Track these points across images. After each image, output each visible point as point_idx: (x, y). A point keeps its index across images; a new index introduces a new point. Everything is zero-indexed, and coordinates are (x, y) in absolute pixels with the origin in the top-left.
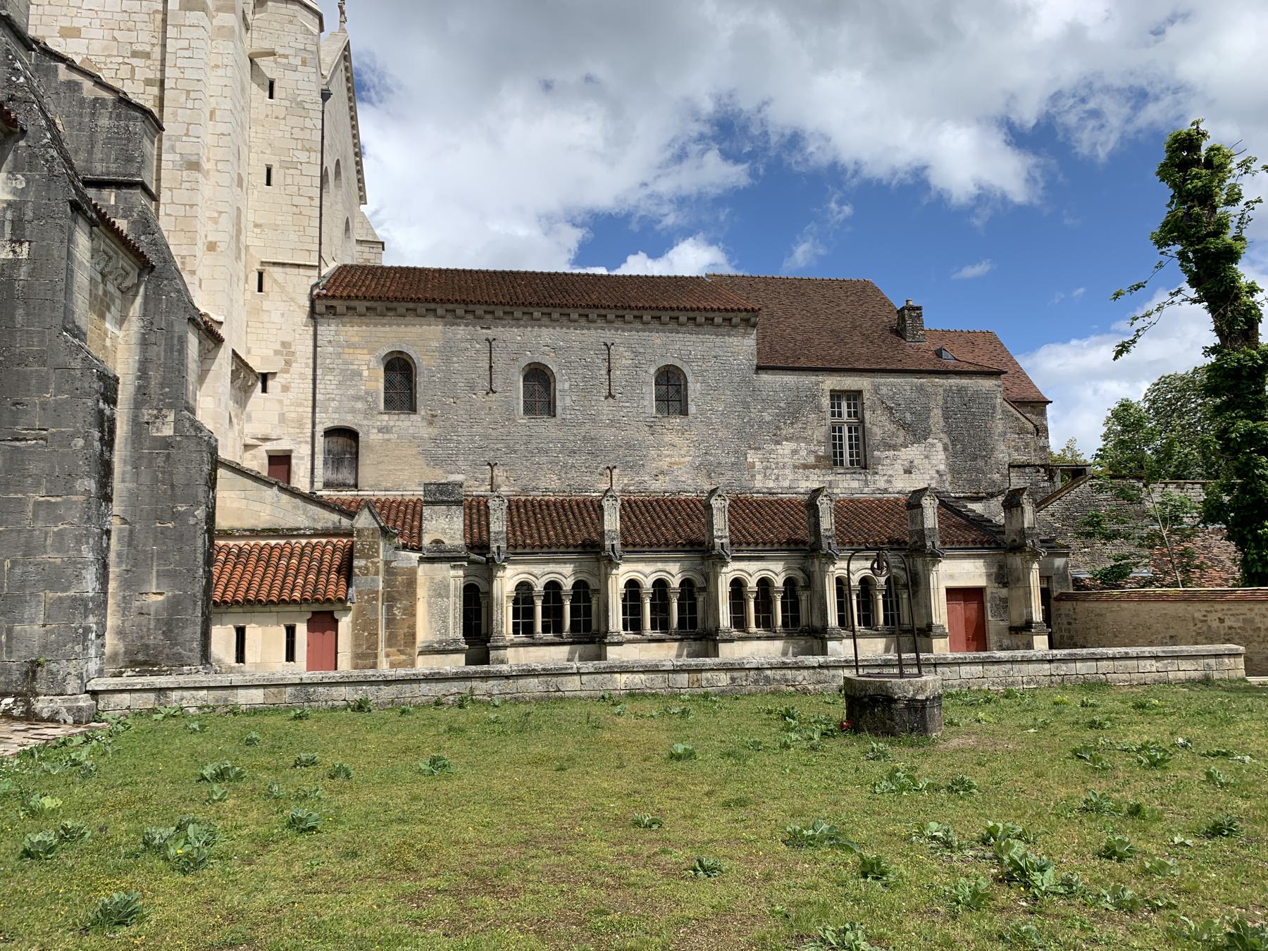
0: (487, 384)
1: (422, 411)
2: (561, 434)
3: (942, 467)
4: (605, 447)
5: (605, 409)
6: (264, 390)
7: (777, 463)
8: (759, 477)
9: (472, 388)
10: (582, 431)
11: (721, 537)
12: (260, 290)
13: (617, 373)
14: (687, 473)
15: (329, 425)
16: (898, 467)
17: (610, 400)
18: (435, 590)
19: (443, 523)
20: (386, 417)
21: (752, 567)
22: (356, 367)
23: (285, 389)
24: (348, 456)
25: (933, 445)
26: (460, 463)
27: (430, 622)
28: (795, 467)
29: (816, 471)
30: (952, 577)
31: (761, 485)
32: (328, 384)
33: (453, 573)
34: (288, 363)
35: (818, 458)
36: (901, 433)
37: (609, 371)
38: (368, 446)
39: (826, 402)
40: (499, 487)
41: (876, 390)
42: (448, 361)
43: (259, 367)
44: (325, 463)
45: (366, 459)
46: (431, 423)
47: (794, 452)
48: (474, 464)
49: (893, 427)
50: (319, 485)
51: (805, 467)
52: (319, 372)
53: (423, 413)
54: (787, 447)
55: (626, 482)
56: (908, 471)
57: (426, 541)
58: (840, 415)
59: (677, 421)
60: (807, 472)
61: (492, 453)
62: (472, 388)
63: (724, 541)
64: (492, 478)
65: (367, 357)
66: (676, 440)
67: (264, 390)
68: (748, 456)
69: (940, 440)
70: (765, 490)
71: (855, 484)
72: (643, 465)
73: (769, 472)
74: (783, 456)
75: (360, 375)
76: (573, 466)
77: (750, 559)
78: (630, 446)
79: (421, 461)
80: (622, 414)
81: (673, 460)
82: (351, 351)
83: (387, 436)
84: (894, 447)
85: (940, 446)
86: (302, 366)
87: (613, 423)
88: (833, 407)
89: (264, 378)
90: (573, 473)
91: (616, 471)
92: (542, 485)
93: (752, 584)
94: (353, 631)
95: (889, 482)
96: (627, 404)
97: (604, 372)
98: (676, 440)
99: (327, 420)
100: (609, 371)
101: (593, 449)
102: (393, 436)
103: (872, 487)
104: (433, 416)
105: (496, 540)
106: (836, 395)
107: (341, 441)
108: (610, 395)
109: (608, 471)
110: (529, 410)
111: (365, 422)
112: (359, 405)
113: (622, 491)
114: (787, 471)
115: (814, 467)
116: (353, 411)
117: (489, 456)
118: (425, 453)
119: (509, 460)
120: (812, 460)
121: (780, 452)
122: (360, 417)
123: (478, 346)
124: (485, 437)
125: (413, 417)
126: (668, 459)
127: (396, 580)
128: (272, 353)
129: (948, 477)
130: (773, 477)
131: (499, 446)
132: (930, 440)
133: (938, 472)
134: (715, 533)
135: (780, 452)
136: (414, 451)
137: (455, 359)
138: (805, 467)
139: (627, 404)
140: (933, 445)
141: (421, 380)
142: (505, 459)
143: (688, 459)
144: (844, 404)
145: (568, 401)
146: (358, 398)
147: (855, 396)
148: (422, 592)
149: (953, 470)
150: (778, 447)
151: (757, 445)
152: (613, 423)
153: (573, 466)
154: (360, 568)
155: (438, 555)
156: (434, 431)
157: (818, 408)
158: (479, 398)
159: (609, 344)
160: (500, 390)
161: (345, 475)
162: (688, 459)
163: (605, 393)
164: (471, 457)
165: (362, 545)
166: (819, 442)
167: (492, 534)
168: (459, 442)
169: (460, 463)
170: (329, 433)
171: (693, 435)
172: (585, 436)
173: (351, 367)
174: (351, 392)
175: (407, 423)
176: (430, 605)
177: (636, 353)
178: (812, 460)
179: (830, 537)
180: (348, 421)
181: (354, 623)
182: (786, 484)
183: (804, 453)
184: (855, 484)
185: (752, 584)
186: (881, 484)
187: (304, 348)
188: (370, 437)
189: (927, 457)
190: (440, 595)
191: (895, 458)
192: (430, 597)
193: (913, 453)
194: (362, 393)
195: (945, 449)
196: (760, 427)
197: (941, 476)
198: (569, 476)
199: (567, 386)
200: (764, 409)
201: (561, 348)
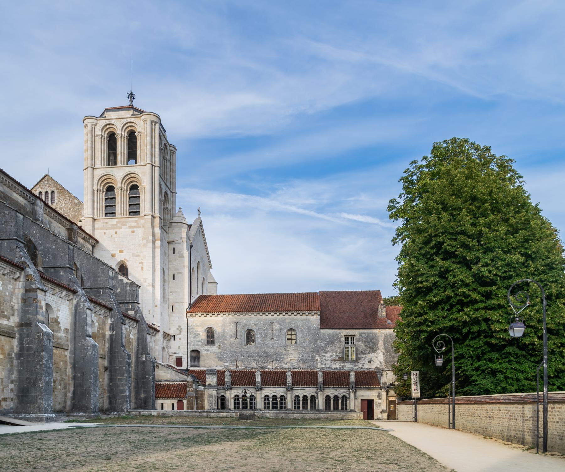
0: (235, 336)
2: (257, 351)
3: (382, 361)
5: (271, 343)
6: (174, 340)
8: (319, 364)
10: (263, 350)
12: (173, 311)
13: (274, 332)
15: (192, 349)
16: (367, 360)
17: (273, 340)
20: (206, 347)
21: (301, 392)
23: (180, 339)
25: (379, 353)
28: (331, 361)
29: (338, 362)
30: (363, 396)
32: (191, 337)
33: (214, 392)
34: (180, 332)
35: (339, 358)
36: (368, 349)
38: (202, 355)
39: (343, 339)
40: (238, 367)
41: (360, 334)
43: (171, 333)
44: (191, 360)
45: (202, 359)
46: (219, 348)
47: (331, 356)
48: (231, 360)
49: (365, 347)
50: (189, 366)
51: (335, 360)
52: (189, 334)
53: (217, 345)
54: (329, 354)
56: (370, 362)
57: (207, 384)
58: (348, 343)
60: (335, 362)
65: (202, 329)
66: (293, 352)
67: (174, 340)
69: (382, 351)
71: (351, 366)
73: (322, 362)
74: (328, 357)
75: (199, 334)
76: (260, 361)
77: (301, 390)
78: (278, 354)
79: (217, 360)
83: (207, 352)
84: (365, 354)
85: (381, 354)
86: (184, 332)
87: (273, 347)
88: (346, 340)
89: (174, 336)
91: (274, 362)
92: (251, 366)
93: (301, 397)
95: (363, 365)
97: (270, 331)
98: (293, 352)
99: (192, 348)
101: (267, 355)
102: (209, 352)
103: (357, 367)
106: (346, 337)
107: (195, 354)
108: (272, 339)
111: (201, 348)
112: (200, 343)
113: (276, 368)
114: (329, 362)
115: (338, 360)
116: (198, 345)
118: (218, 357)
120: (337, 358)
121: (327, 356)
122: (200, 347)
124: (235, 352)
126: (290, 358)
128: (176, 329)
129: (384, 364)
132: (378, 352)
133: (380, 362)
135: (327, 356)
136: (215, 356)
138: (335, 360)
140: (379, 353)
142: (240, 359)
143: (297, 358)
144: (350, 339)
145: (259, 341)
146: (199, 341)
147: (353, 337)
148: (206, 397)
149: (386, 362)
152: (273, 347)
155: (210, 387)
156: (220, 351)
157: (340, 341)
158: (233, 340)
161: (196, 363)
163: (270, 337)
166: (340, 353)
168: (227, 354)
170: (192, 351)
171: (298, 350)
174: (197, 340)
175: (213, 348)
176: (208, 400)
177: (281, 325)
178: (337, 358)
180: (197, 348)
181: (187, 403)
182: (328, 366)
183: (335, 356)
184: (351, 366)
185: (301, 397)
186: (360, 366)
187: (184, 328)
188: (203, 353)
189: (377, 357)
190: (210, 398)
191: (366, 358)
193: (372, 356)
195: (384, 354)
196: (320, 348)
197: (381, 363)
199: (259, 336)
201: (257, 324)
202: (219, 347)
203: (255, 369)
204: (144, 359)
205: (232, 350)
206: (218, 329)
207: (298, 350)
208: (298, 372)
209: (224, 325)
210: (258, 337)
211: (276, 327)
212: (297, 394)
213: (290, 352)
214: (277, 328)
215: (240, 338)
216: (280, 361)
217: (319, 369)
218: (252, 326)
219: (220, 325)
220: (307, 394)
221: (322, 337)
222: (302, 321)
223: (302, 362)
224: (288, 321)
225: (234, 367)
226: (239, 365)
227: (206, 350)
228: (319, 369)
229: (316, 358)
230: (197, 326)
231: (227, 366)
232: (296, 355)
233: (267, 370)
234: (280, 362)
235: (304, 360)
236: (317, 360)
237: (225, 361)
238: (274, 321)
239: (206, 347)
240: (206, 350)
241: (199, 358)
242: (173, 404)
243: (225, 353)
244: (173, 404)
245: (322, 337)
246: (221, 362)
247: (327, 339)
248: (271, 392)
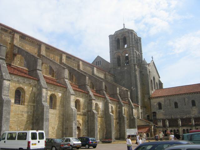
42: (165, 103)
45: (157, 116)
108: (185, 105)
116: (155, 110)
141: (162, 106)
202: (164, 110)
204: (132, 118)
206: (163, 103)
209: (165, 101)
219: (163, 101)
227: (159, 112)
239: (159, 111)
240: (159, 112)
241: (156, 115)
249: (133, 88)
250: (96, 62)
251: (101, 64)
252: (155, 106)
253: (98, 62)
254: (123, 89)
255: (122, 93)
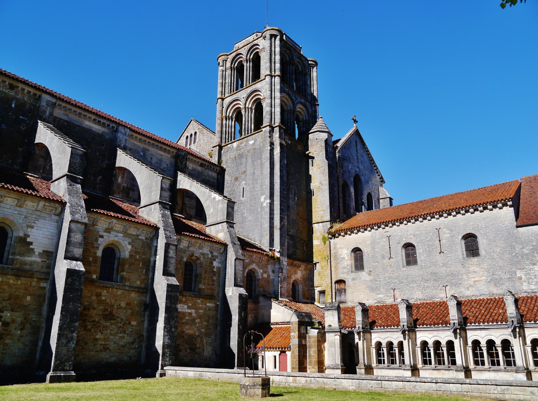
1: (366, 269)
2: (421, 273)
4: (441, 276)
5: (440, 258)
7: (535, 276)
9: (383, 257)
11: (453, 320)
14: (484, 285)
18: (330, 344)
19: (331, 317)
20: (353, 274)
22: (343, 256)
24: (343, 290)
26: (381, 290)
27: (329, 357)
31: (527, 288)
37: (440, 241)
42: (373, 248)
46: (370, 275)
55: (453, 292)
59: (475, 260)
61: (393, 284)
62: (383, 257)
63: (455, 321)
64: (394, 295)
68: (517, 273)
70: (530, 291)
72: (461, 283)
73: (531, 281)
76: (428, 287)
80: (448, 260)
81: (476, 279)
82: (341, 250)
83: (355, 282)
87: (444, 265)
90: (428, 290)
94: (291, 358)
96: (450, 255)
97: (438, 242)
98: (477, 269)
100: (440, 241)
101: (436, 277)
102: (357, 281)
104: (370, 271)
105: (359, 324)
109: (444, 288)
110: (409, 263)
112: (345, 270)
116: (343, 273)
117: (392, 286)
119: (400, 287)
123: (384, 240)
124: (390, 278)
125: (363, 273)
126: (473, 279)
127: (310, 340)
130: (534, 283)
131: (396, 281)
134: (451, 318)
137: (376, 247)
139: (450, 255)
143: (484, 278)
145: (422, 257)
150: (535, 266)
151: (522, 267)
152: (444, 265)
153: (428, 287)
154: (292, 336)
159: (438, 229)
160: (393, 257)
162: (484, 278)
164: (385, 287)
165: (293, 328)
167: (357, 322)
168: (380, 281)
169: (381, 290)
171: (485, 265)
172: (432, 273)
173: (341, 256)
176: (328, 350)
177: (452, 231)
179: (513, 317)
180: (341, 277)
188: (349, 282)
192: (329, 347)
194: (346, 266)
196: (522, 257)
198: (426, 292)
199: (421, 251)
200: (523, 248)
202: (370, 272)
203: (420, 300)
205: (386, 275)
207: (485, 265)
208: (488, 299)
209: (374, 243)
210: (420, 253)
211: (445, 235)
212: (475, 338)
213: (472, 269)
214: (446, 236)
215: (396, 257)
216: (457, 285)
217: (525, 292)
218: (410, 238)
220: (493, 338)
221: (523, 240)
222: (484, 219)
223: (493, 283)
224: (462, 223)
225: (391, 300)
226: (397, 296)
227: (354, 279)
228: (525, 292)
229: (518, 275)
230: (342, 248)
231: (381, 298)
232: (482, 273)
233: (438, 300)
234: (458, 287)
235: (496, 279)
236: (520, 278)
237: (379, 292)
238: (441, 227)
239: (353, 275)
242: (275, 357)
243: (377, 281)
244: (275, 357)
245: (523, 240)
246: (374, 294)
247: (532, 241)
248: (430, 336)
249: (265, 199)
250: (187, 137)
251: (197, 140)
252: (344, 258)
253: (191, 135)
254: (214, 198)
255: (212, 211)
